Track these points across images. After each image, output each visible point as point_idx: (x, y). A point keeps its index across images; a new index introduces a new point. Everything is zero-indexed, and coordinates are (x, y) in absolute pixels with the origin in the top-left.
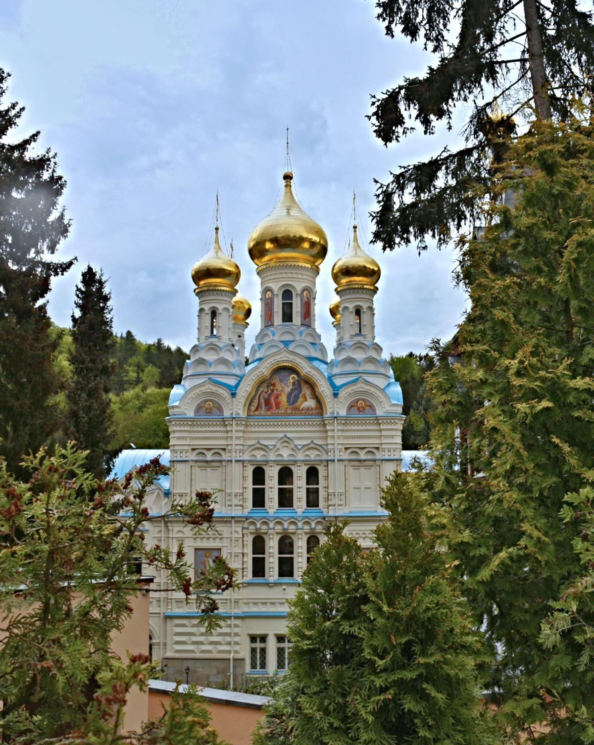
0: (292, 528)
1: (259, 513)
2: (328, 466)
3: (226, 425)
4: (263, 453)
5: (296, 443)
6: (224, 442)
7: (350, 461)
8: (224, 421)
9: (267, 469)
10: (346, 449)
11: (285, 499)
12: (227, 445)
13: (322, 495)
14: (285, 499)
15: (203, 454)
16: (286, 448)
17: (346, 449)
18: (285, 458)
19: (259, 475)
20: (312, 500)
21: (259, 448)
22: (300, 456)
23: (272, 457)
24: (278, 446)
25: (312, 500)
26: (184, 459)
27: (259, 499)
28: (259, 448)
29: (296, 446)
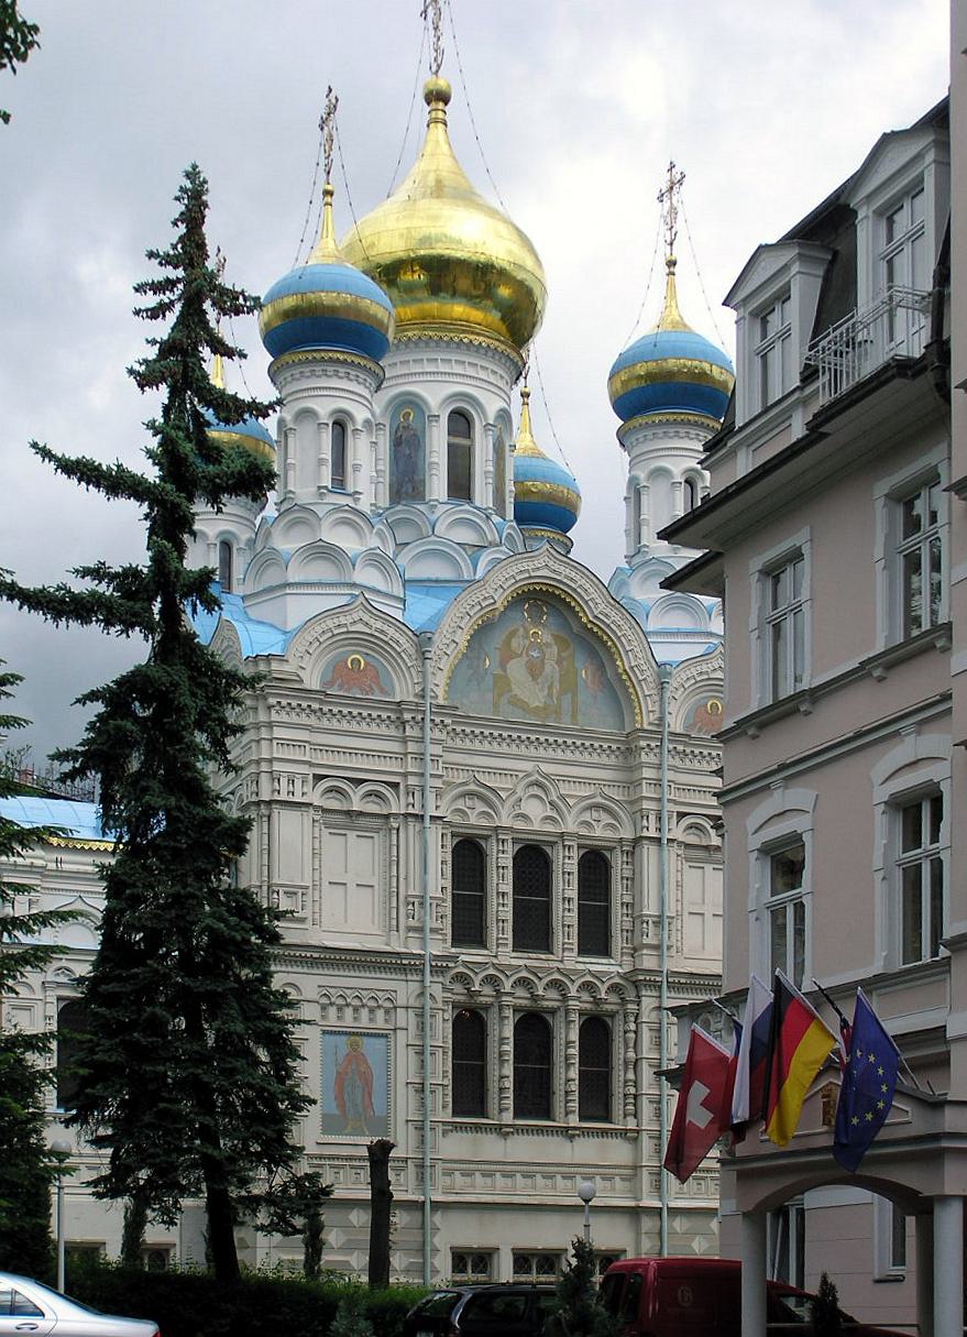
0: (551, 999)
1: (470, 955)
2: (633, 853)
3: (404, 723)
4: (480, 807)
5: (562, 792)
6: (395, 767)
7: (688, 846)
8: (401, 712)
9: (492, 848)
10: (682, 815)
11: (533, 930)
12: (405, 775)
13: (619, 919)
14: (533, 930)
15: (378, 795)
16: (535, 802)
17: (682, 815)
18: (536, 827)
19: (469, 856)
20: (595, 938)
21: (472, 794)
22: (570, 825)
23: (505, 819)
24: (520, 792)
25: (595, 938)
26: (297, 798)
27: (469, 925)
28: (472, 794)
29: (562, 798)
